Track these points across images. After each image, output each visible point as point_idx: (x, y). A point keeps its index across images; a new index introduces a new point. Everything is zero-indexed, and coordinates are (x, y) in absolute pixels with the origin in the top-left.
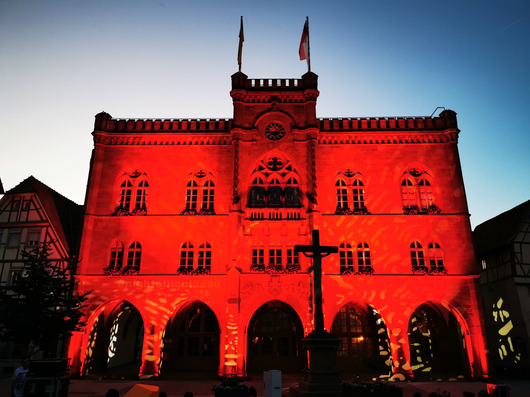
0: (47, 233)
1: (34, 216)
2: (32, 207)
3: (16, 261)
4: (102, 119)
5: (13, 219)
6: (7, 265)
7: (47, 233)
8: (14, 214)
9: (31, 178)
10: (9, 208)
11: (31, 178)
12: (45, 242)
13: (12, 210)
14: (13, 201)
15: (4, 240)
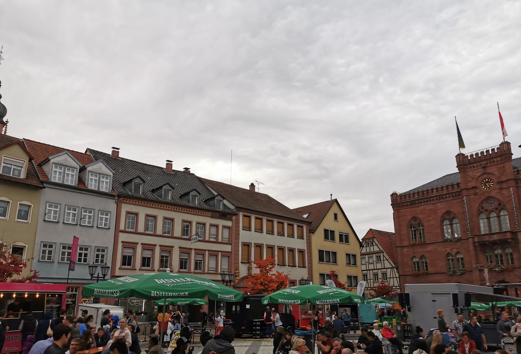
0: (383, 256)
1: (376, 249)
2: (374, 244)
3: (374, 269)
4: (394, 196)
5: (368, 251)
6: (371, 271)
7: (383, 256)
8: (368, 248)
9: (371, 229)
10: (365, 246)
11: (371, 229)
12: (384, 260)
13: (366, 247)
14: (366, 242)
15: (367, 261)
